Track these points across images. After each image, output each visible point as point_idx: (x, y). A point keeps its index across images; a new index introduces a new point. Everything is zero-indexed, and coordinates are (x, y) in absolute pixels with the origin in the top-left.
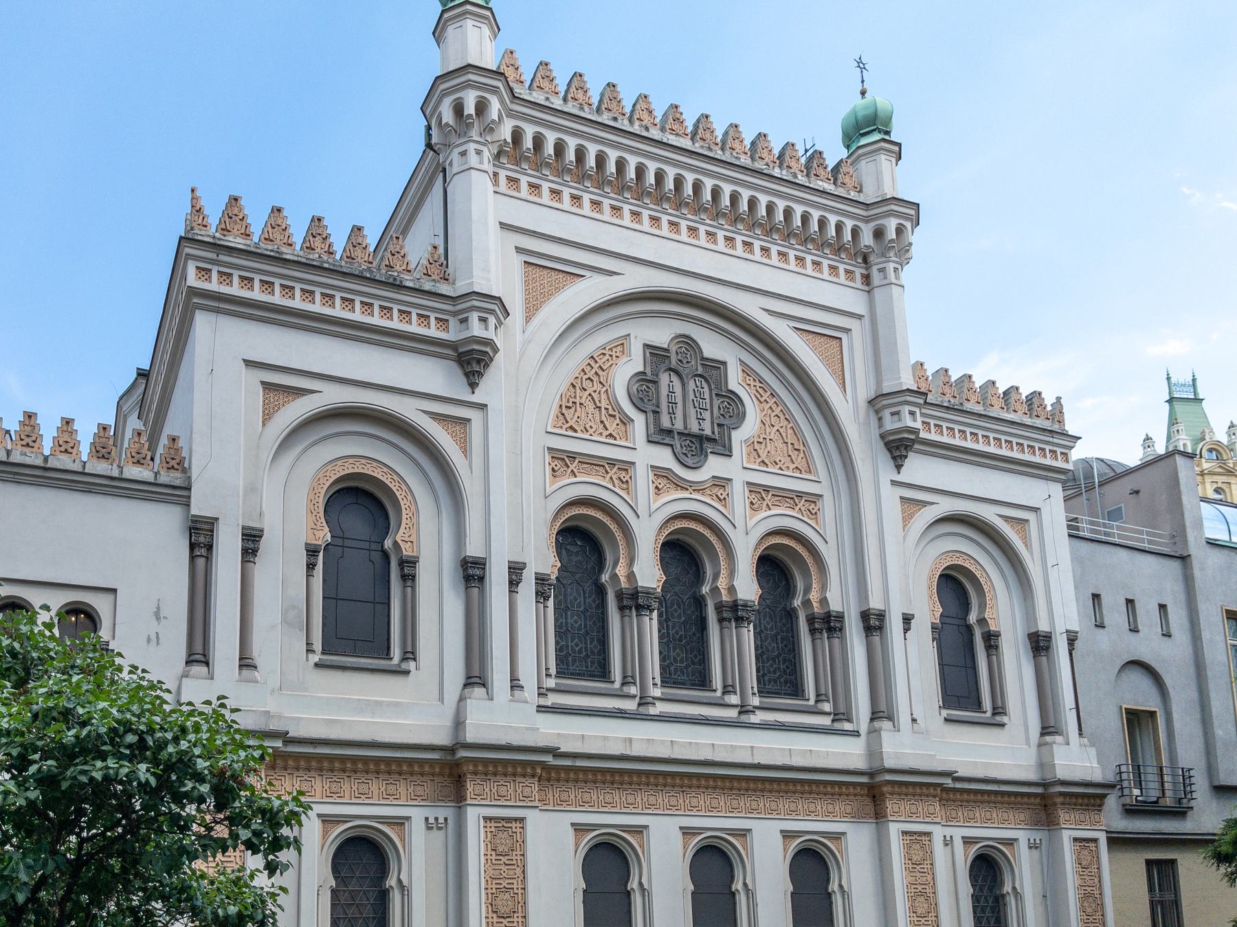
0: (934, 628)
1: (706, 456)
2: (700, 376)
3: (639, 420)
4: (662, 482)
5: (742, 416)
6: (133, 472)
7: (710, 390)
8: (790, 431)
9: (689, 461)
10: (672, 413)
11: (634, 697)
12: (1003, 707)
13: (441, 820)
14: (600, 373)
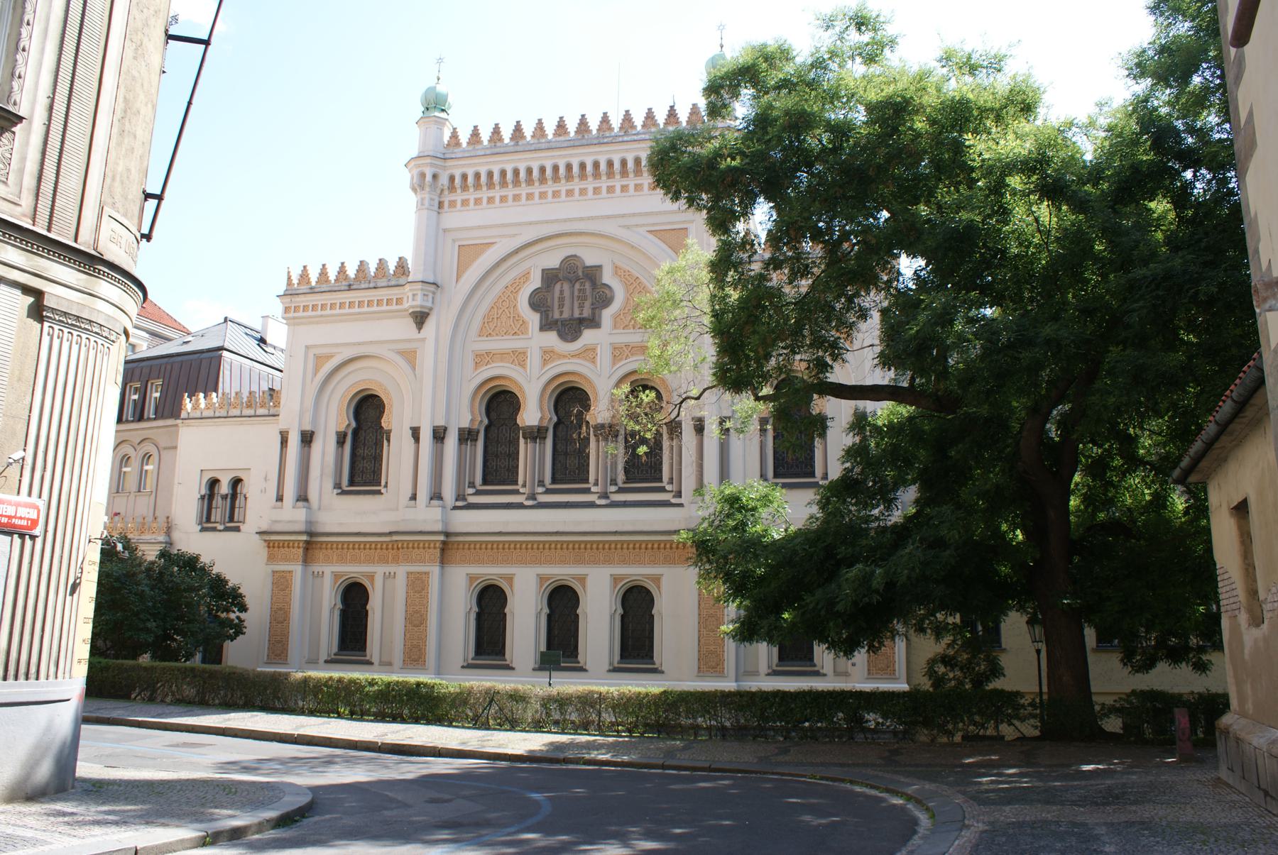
3: (534, 319)
4: (547, 357)
6: (261, 411)
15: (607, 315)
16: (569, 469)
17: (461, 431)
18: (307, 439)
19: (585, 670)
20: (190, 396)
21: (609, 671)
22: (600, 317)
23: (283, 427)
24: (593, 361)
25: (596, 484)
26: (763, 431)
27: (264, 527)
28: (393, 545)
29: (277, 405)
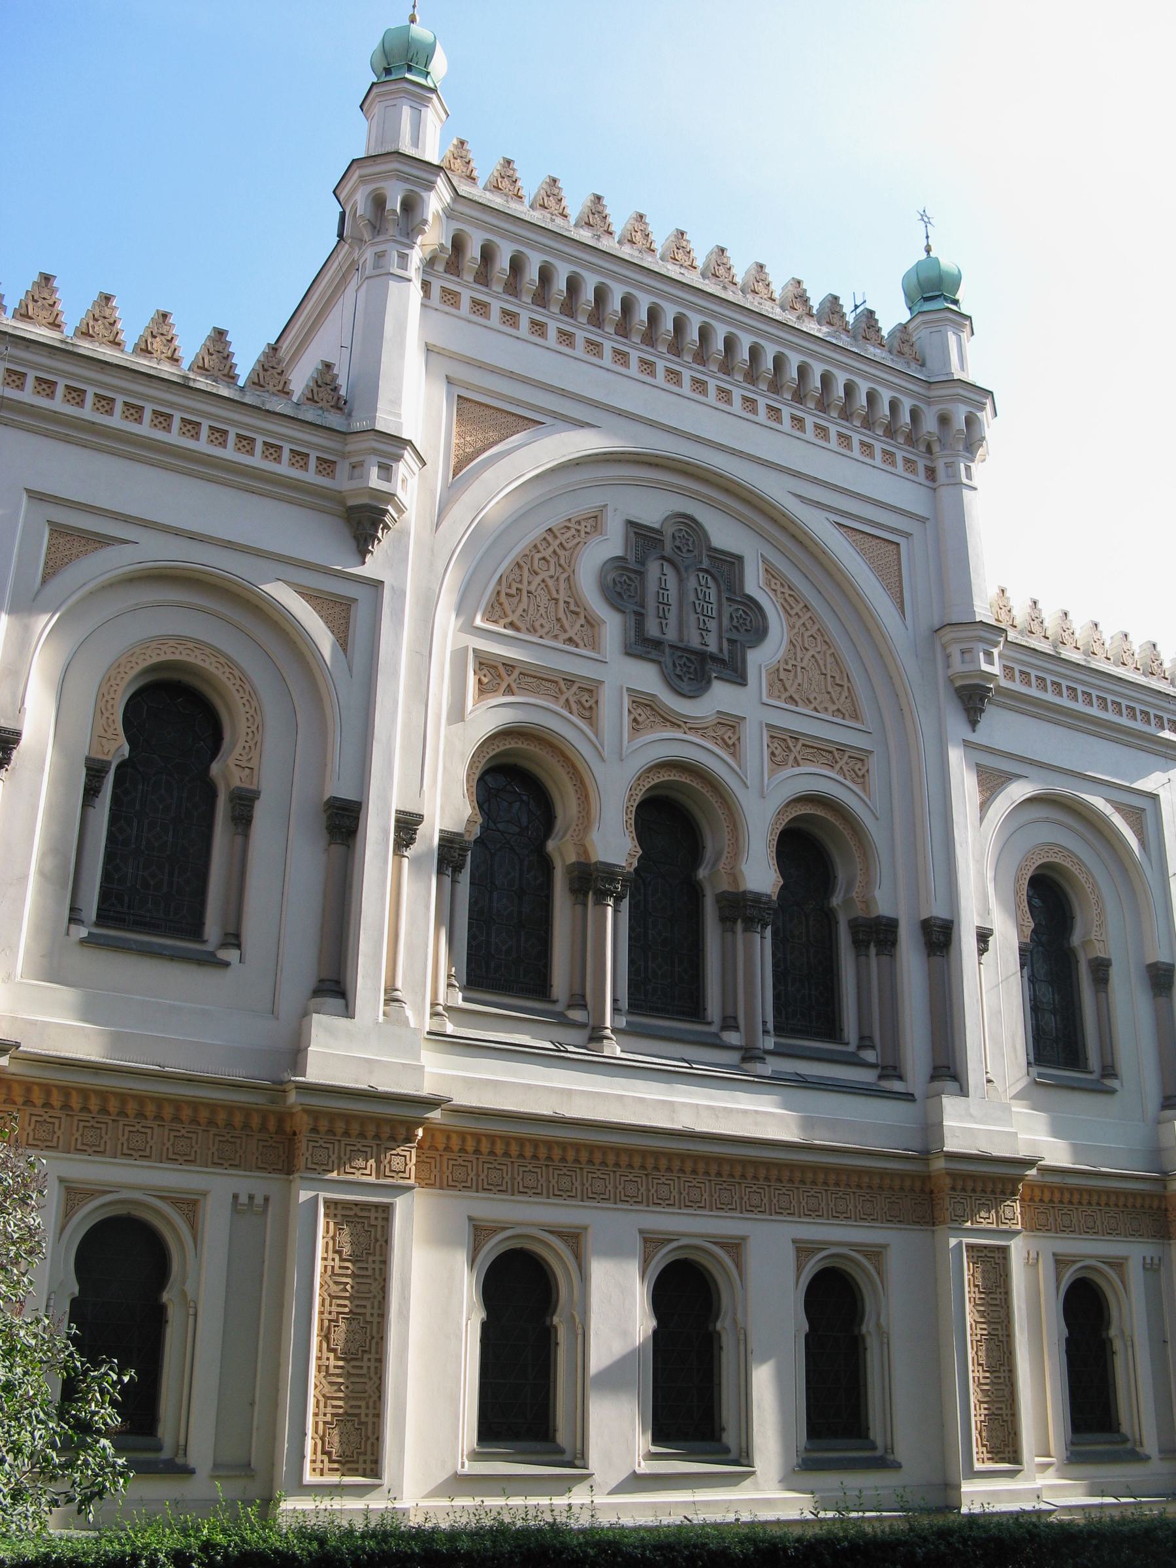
1: (709, 682)
2: (706, 571)
3: (612, 626)
4: (643, 715)
5: (760, 633)
7: (719, 591)
8: (829, 659)
9: (685, 687)
12: (1113, 1067)
13: (259, 1200)
14: (561, 552)
22: (744, 661)
26: (1022, 968)
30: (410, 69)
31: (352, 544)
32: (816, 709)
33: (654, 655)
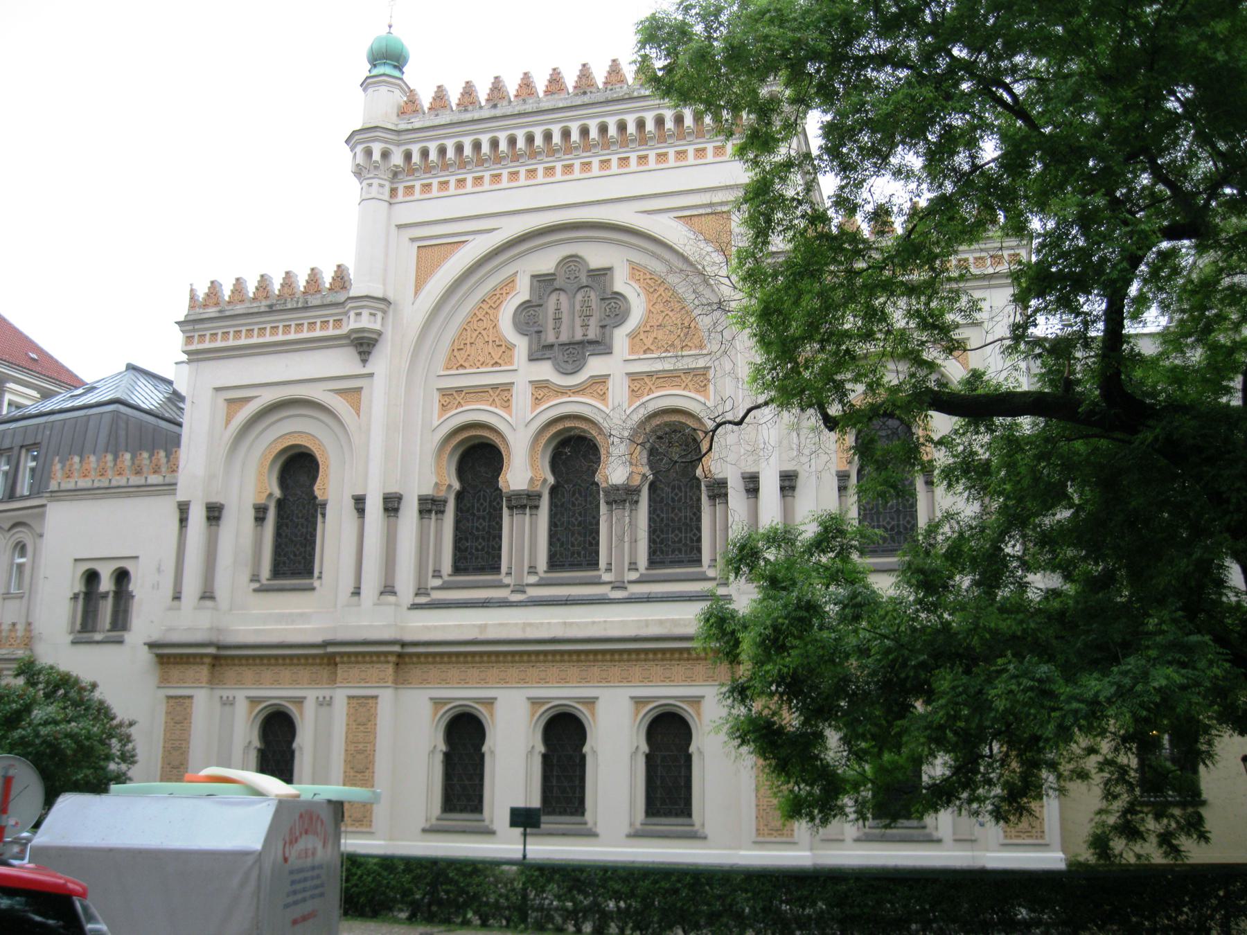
0: (843, 477)
3: (521, 345)
9: (569, 368)
10: (557, 329)
11: (508, 586)
15: (620, 337)
16: (574, 548)
17: (423, 500)
18: (214, 513)
19: (595, 835)
20: (60, 461)
21: (629, 836)
22: (611, 338)
23: (181, 496)
24: (603, 396)
25: (609, 570)
26: (842, 489)
27: (156, 636)
28: (328, 658)
29: (174, 470)
30: (375, 66)
31: (357, 357)
32: (667, 351)
33: (548, 354)
